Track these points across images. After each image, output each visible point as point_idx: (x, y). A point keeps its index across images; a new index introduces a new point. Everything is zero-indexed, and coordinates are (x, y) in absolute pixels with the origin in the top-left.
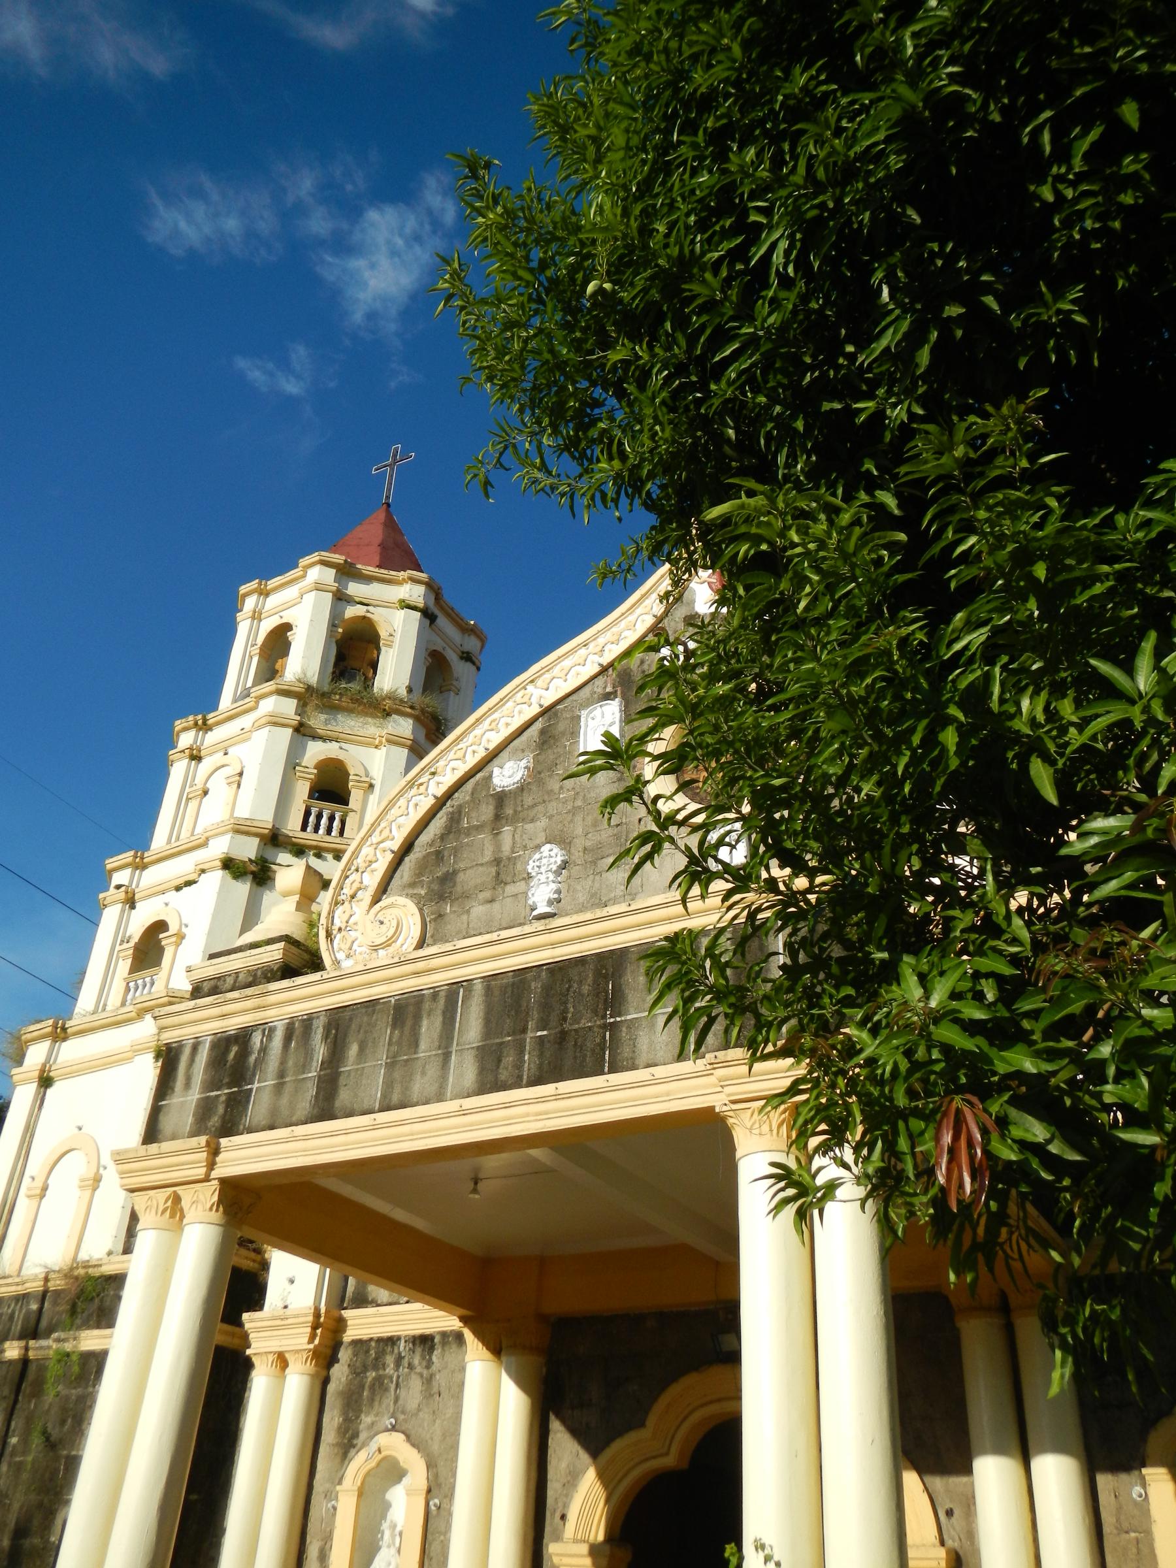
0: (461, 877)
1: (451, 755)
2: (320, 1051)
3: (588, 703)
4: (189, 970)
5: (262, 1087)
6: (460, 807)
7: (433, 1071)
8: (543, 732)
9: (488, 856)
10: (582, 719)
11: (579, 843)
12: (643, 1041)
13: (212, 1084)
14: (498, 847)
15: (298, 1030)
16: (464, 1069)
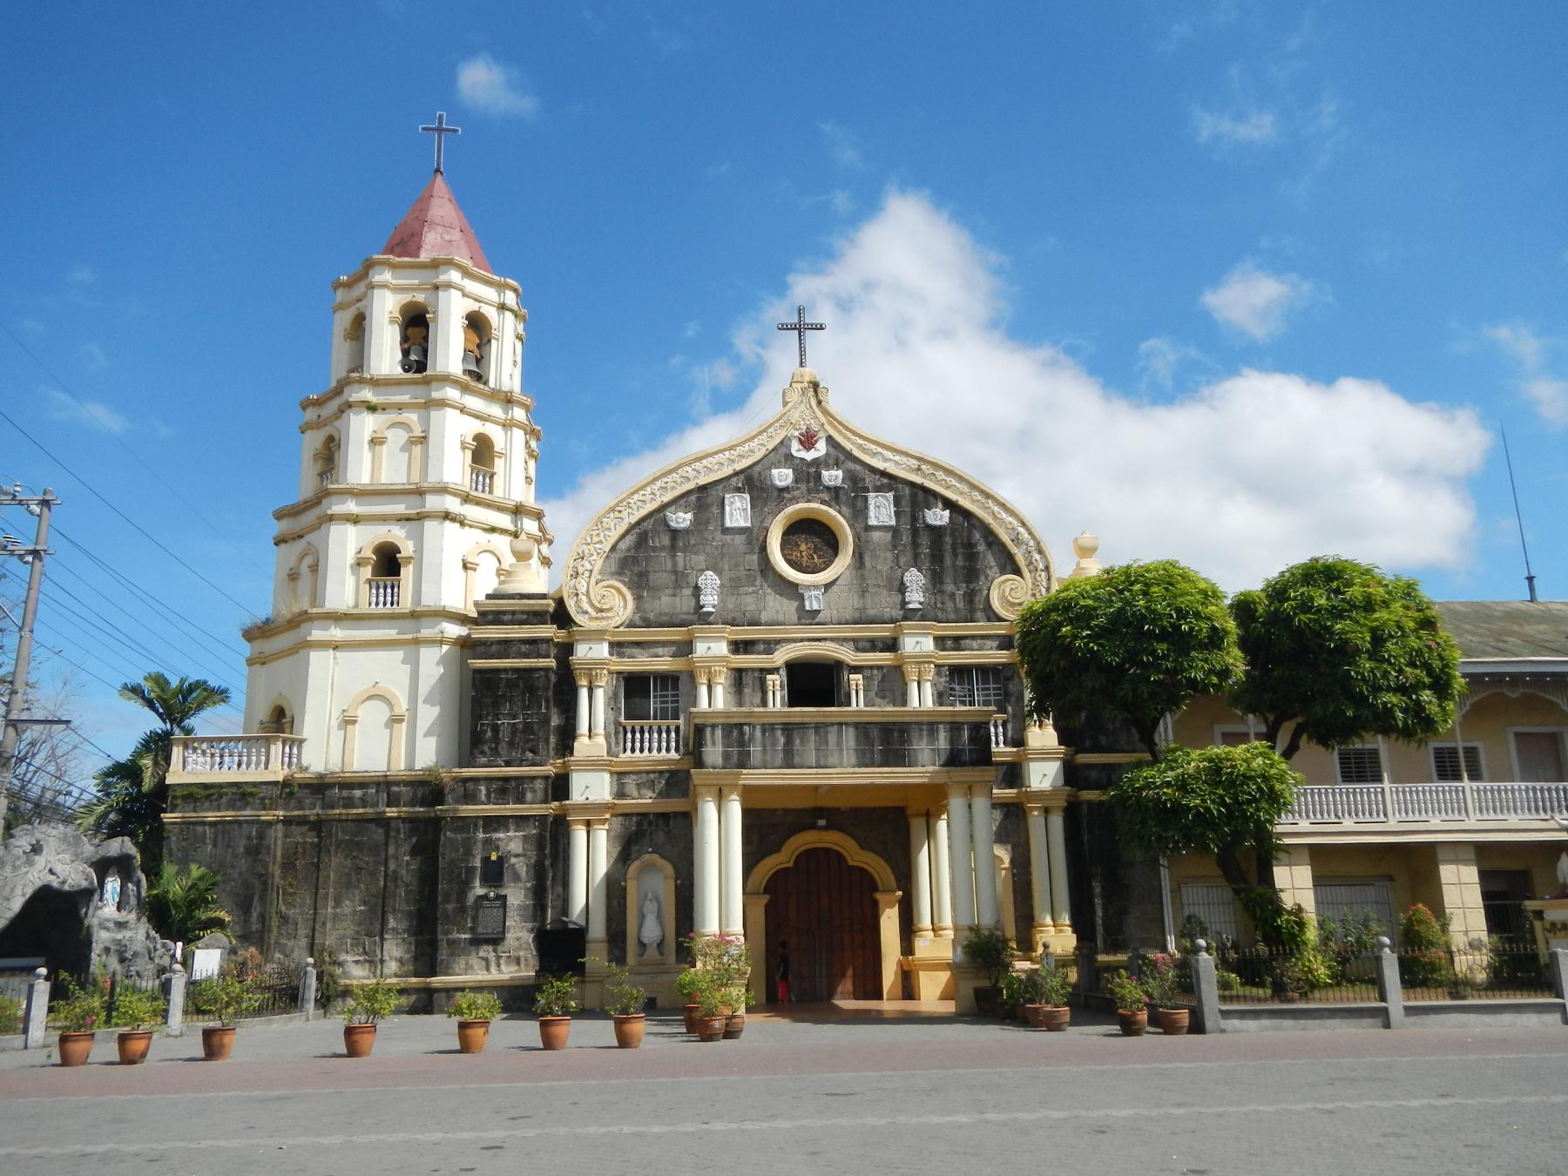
0: (651, 576)
1: (636, 497)
2: (782, 740)
3: (726, 490)
4: (476, 604)
5: (755, 750)
6: (645, 533)
7: (836, 754)
8: (698, 499)
9: (669, 566)
10: (727, 502)
11: (726, 575)
12: (920, 756)
13: (724, 745)
14: (675, 564)
15: (768, 728)
16: (849, 756)
